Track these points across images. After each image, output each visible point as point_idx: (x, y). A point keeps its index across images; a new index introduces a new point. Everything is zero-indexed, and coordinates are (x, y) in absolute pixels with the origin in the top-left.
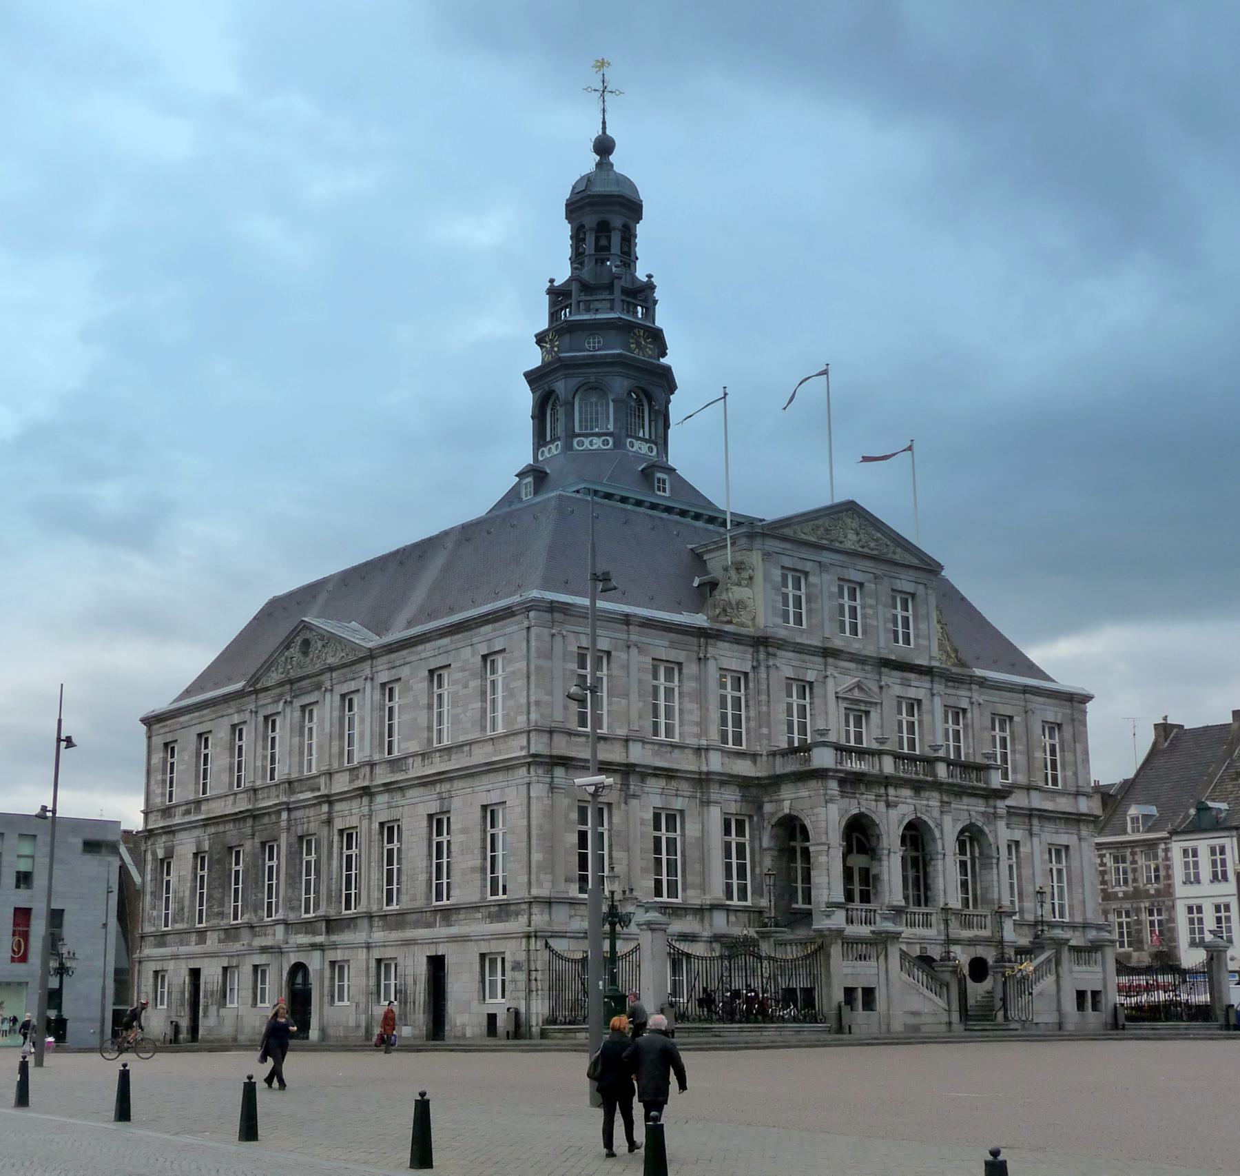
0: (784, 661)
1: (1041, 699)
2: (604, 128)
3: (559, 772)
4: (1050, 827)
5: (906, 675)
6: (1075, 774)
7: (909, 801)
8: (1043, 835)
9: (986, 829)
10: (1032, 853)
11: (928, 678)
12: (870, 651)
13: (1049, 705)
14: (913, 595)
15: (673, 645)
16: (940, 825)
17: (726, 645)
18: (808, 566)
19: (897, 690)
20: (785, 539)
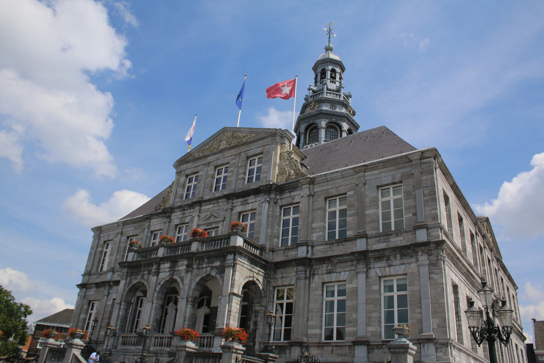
0: (175, 217)
1: (378, 171)
2: (329, 42)
3: (84, 290)
4: (384, 263)
5: (245, 199)
6: (415, 214)
7: (167, 270)
8: (372, 273)
9: (218, 277)
10: (357, 288)
11: (262, 194)
12: (226, 192)
13: (385, 172)
14: (262, 153)
15: (136, 228)
16: (182, 280)
17: (155, 220)
18: (199, 169)
19: (239, 209)
20: (188, 162)
